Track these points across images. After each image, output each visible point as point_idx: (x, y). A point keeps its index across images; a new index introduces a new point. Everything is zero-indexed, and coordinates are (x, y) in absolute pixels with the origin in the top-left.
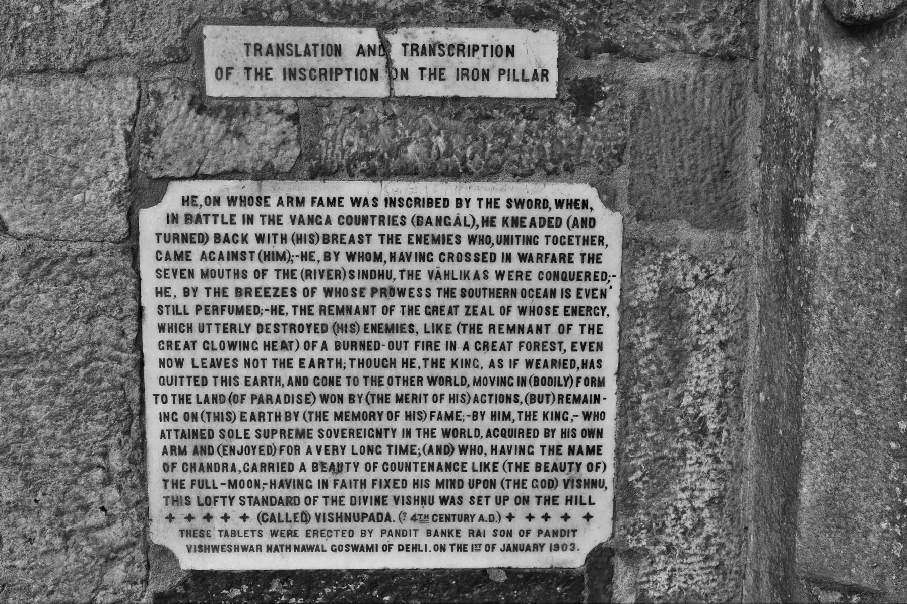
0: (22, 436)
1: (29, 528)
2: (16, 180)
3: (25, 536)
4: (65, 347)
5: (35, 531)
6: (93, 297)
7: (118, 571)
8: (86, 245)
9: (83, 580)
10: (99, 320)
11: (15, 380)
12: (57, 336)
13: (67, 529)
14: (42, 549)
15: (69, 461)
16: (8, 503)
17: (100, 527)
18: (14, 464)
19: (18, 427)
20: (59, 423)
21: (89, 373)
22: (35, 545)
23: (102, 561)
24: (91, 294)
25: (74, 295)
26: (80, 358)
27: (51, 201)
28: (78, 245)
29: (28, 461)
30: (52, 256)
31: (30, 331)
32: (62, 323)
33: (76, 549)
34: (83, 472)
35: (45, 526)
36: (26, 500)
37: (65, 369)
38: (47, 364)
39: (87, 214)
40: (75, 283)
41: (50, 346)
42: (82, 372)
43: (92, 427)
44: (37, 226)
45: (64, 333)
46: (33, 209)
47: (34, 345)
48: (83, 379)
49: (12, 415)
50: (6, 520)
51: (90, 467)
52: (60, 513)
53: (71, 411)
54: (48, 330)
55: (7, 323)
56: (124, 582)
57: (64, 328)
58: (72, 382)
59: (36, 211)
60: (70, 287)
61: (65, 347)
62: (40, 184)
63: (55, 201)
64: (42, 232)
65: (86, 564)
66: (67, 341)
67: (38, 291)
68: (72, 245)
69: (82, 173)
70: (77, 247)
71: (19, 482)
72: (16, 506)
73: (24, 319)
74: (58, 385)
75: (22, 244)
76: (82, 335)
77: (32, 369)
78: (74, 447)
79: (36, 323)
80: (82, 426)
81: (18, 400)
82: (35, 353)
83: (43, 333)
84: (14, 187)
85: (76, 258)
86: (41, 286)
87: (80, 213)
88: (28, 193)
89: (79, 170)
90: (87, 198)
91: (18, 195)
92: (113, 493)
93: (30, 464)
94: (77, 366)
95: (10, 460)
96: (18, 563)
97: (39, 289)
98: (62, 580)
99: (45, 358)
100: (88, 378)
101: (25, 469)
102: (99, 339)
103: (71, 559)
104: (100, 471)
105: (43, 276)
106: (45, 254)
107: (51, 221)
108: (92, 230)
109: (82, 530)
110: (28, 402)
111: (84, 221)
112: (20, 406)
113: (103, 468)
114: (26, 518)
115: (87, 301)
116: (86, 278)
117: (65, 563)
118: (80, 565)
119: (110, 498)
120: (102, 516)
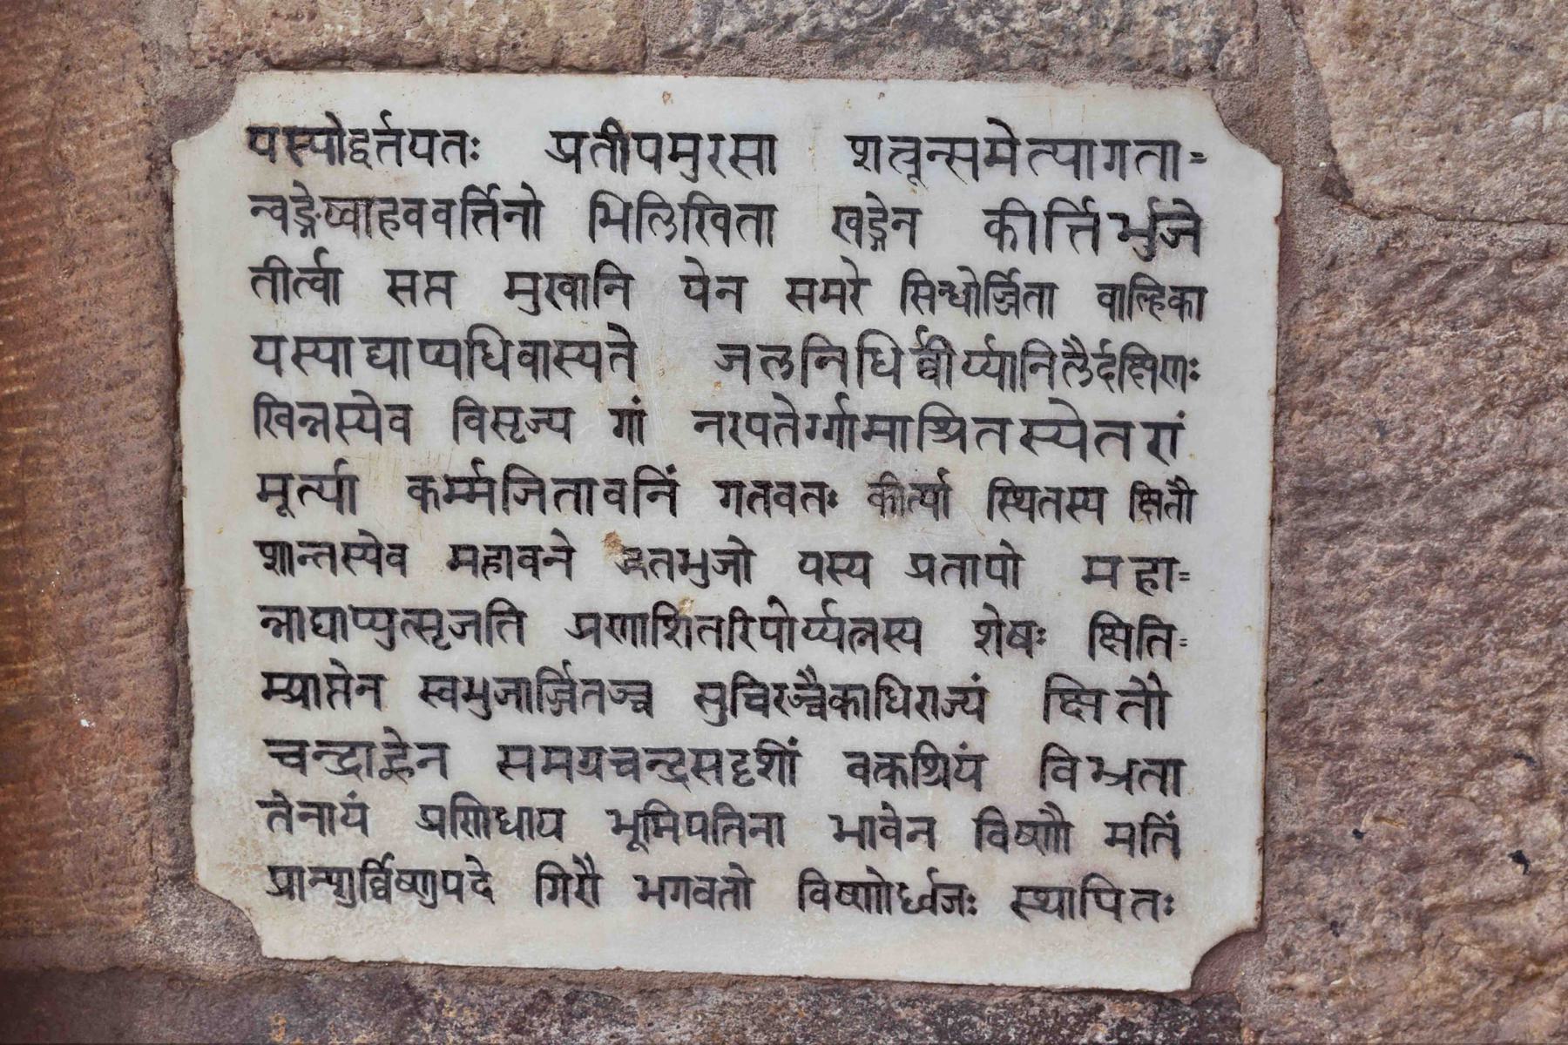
0: (1340, 680)
1: (1335, 897)
2: (1382, 79)
3: (1323, 917)
4: (1464, 471)
5: (1350, 907)
6: (1541, 355)
7: (1539, 1009)
8: (1537, 232)
9: (1450, 1028)
10: (1549, 411)
11: (1335, 548)
12: (1445, 447)
13: (1427, 902)
14: (1362, 948)
15: (1449, 741)
16: (1291, 837)
17: (1508, 902)
18: (1315, 745)
19: (1333, 657)
20: (1433, 651)
21: (1517, 534)
22: (1344, 938)
23: (1506, 980)
24: (1537, 348)
25: (1495, 351)
26: (1499, 499)
27: (1457, 130)
28: (1518, 233)
29: (1347, 739)
30: (1452, 257)
31: (1384, 433)
32: (1460, 417)
33: (1444, 950)
34: (1480, 767)
35: (1373, 893)
36: (1335, 830)
37: (1460, 523)
38: (1416, 512)
39: (1547, 160)
40: (1500, 324)
41: (1427, 470)
42: (1498, 533)
43: (1513, 663)
44: (1423, 186)
45: (1463, 440)
46: (1415, 148)
47: (1388, 468)
48: (1503, 549)
49: (1321, 631)
50: (1281, 877)
51: (1498, 757)
52: (1414, 865)
53: (1465, 622)
54: (1425, 431)
55: (1325, 416)
56: (1555, 1035)
57: (1464, 426)
58: (1474, 555)
59: (1424, 152)
60: (1487, 331)
61: (1464, 471)
62: (1437, 91)
63: (1467, 127)
64: (1434, 201)
65: (1465, 989)
66: (1470, 457)
67: (1410, 341)
68: (1502, 232)
69: (1540, 64)
70: (1516, 237)
71: (1319, 788)
72: (1310, 845)
73: (1370, 404)
74: (1439, 561)
75: (1383, 231)
76: (1506, 445)
77: (1379, 522)
78: (1461, 710)
79: (1398, 415)
80: (1485, 660)
81: (1337, 594)
82: (1389, 485)
83: (1414, 439)
84: (1376, 96)
85: (1509, 262)
86: (1417, 329)
87: (1530, 158)
88: (1407, 110)
89: (1532, 57)
90: (1547, 122)
91: (1382, 113)
92: (1544, 821)
93: (1352, 747)
94: (1490, 518)
95: (1306, 736)
96: (1300, 980)
97: (1412, 334)
98: (1403, 1025)
99: (1414, 497)
100: (1513, 547)
101: (1340, 756)
102: (1549, 455)
103: (1430, 976)
104: (1520, 769)
105: (1426, 305)
106: (1436, 252)
107: (1457, 175)
108: (1556, 198)
109: (1460, 907)
110: (1361, 599)
111: (1538, 175)
112: (1341, 609)
113: (1529, 760)
114: (1329, 873)
115: (1525, 363)
116: (1530, 310)
117: (1414, 985)
118: (1451, 989)
119: (1537, 833)
120: (1513, 876)
